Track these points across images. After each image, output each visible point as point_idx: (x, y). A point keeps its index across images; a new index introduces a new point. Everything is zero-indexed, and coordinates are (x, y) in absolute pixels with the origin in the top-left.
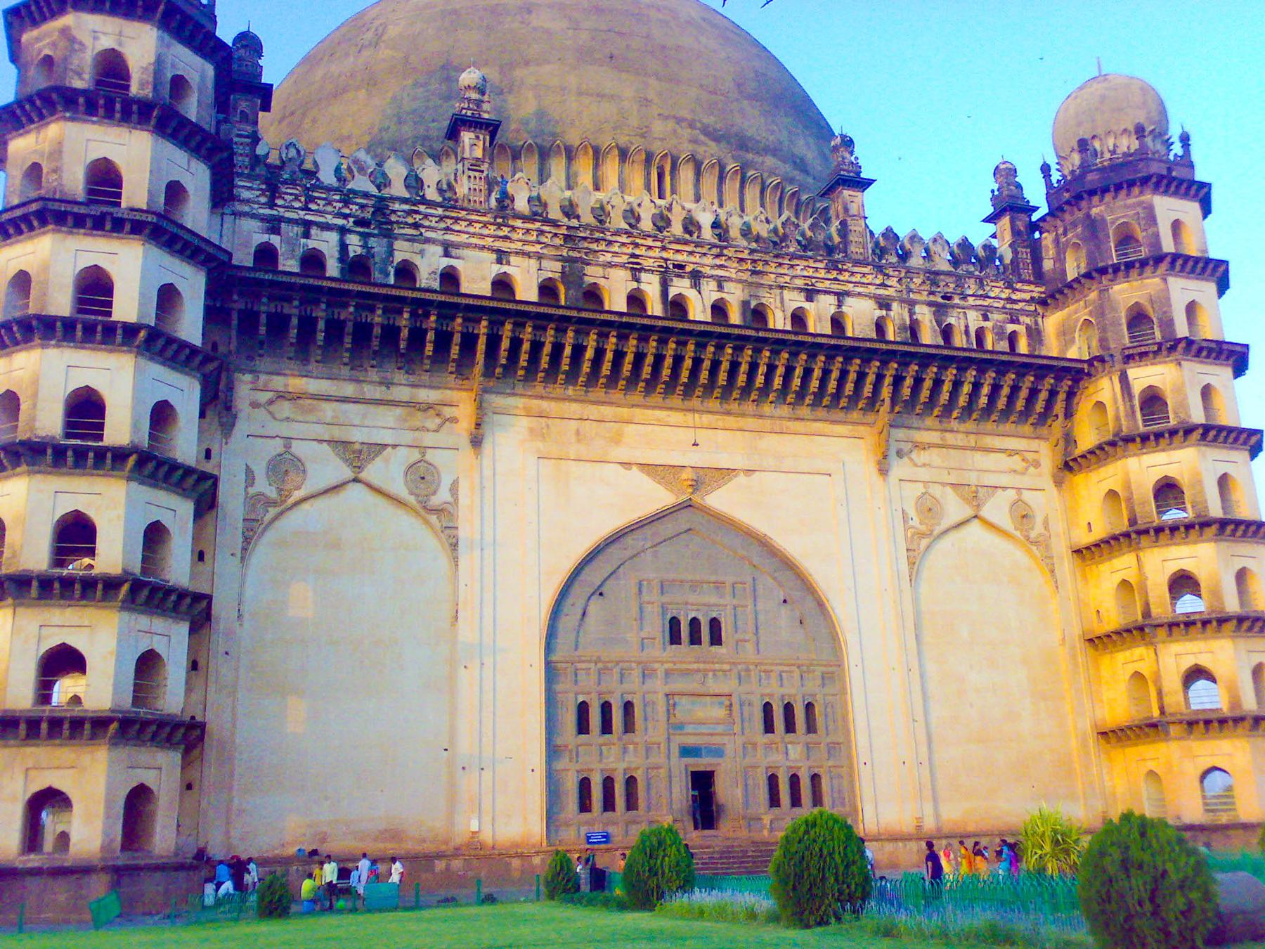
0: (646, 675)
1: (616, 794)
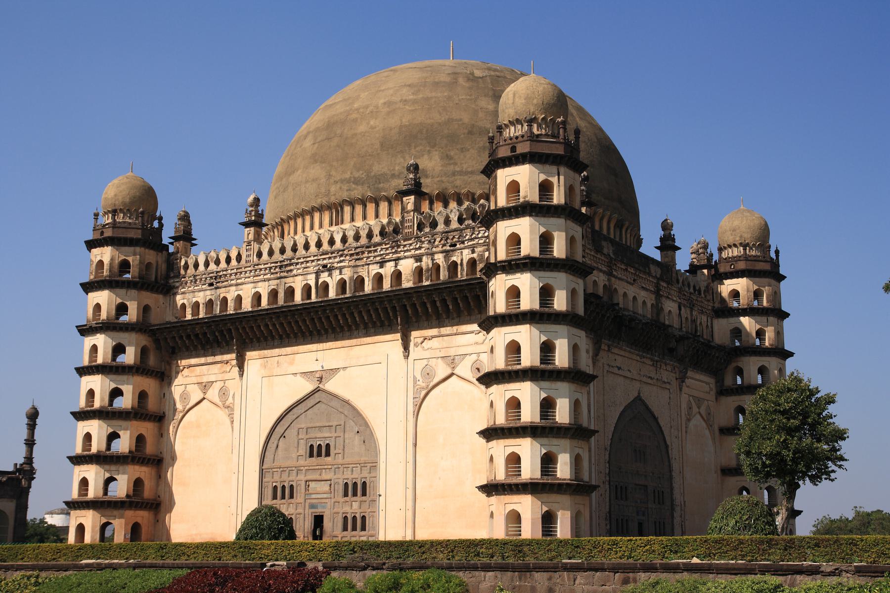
0: (299, 471)
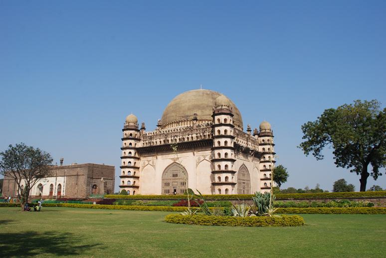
1: (168, 191)
